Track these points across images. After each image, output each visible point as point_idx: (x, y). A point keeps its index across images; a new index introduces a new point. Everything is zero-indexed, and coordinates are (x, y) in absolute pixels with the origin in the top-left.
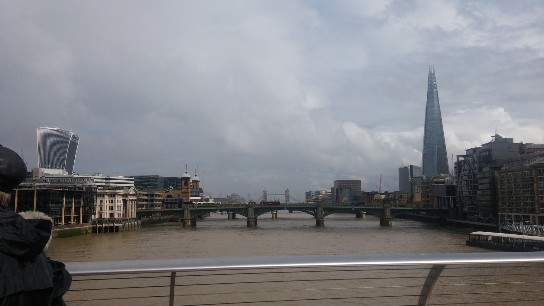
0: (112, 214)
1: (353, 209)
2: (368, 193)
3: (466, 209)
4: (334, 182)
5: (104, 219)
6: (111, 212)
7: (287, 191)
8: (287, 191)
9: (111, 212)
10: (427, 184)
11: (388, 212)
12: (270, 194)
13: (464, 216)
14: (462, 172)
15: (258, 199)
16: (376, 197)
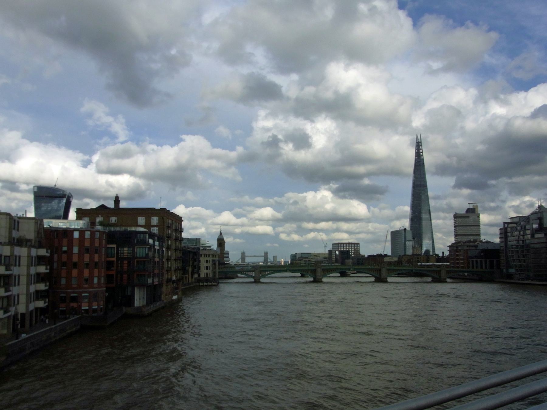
0: (207, 274)
1: (414, 271)
2: (373, 256)
3: (512, 271)
4: (333, 244)
5: (202, 278)
6: (206, 271)
7: (266, 254)
8: (266, 254)
9: (206, 271)
10: (457, 247)
11: (443, 272)
12: (247, 256)
13: (510, 276)
14: (509, 239)
15: (260, 261)
16: (386, 259)
